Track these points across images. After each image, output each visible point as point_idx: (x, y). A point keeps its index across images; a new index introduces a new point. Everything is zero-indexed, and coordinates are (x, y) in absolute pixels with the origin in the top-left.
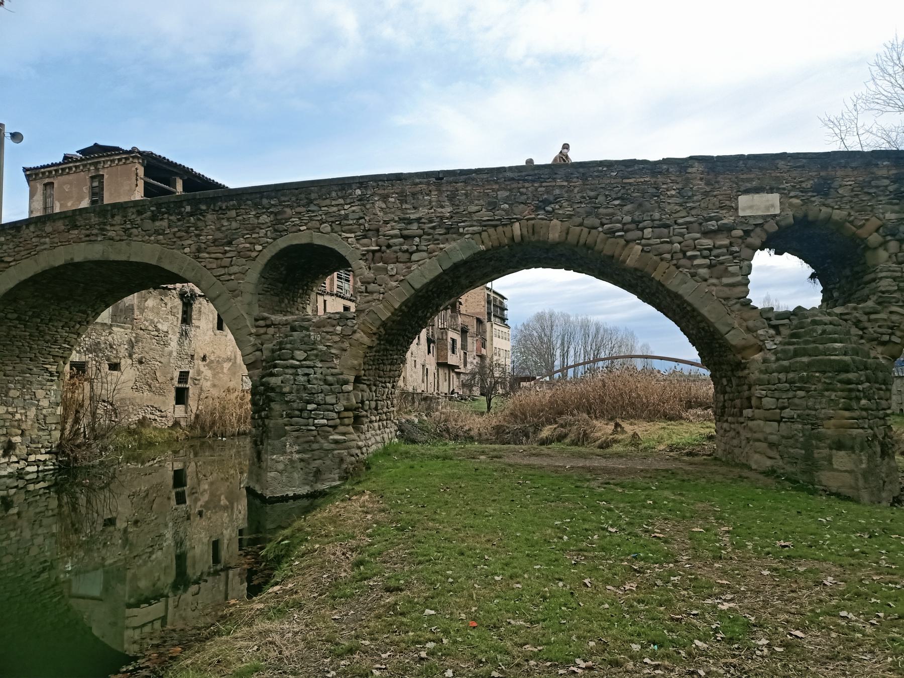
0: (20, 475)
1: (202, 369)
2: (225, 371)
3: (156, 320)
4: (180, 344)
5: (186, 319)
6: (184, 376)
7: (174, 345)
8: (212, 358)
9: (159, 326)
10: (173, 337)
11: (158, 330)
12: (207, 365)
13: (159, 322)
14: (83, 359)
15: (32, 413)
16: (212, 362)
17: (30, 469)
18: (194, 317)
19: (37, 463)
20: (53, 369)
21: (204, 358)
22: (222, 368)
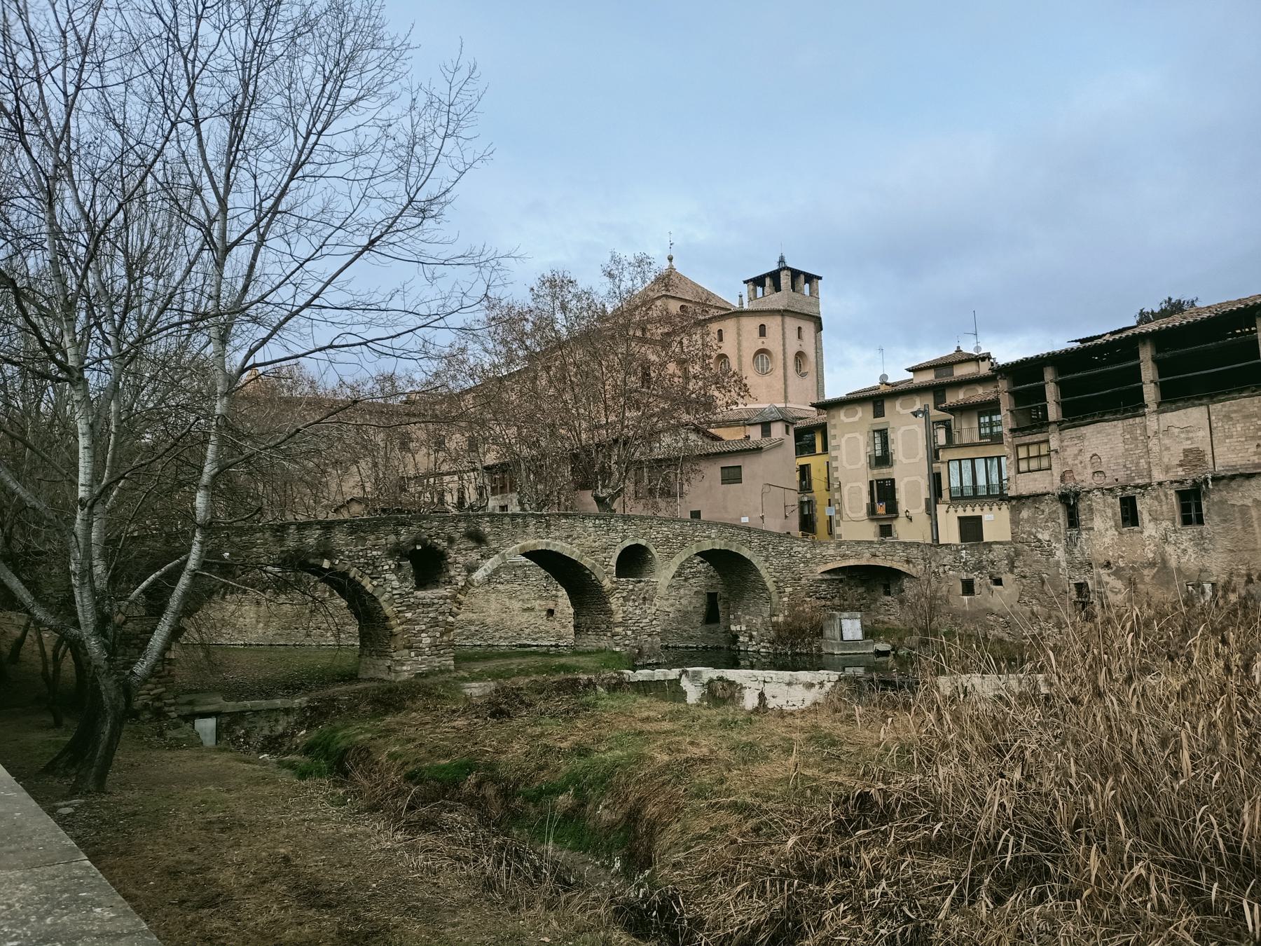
0: (758, 652)
1: (1106, 578)
2: (1147, 579)
3: (1034, 530)
4: (1069, 552)
5: (1073, 521)
6: (1081, 587)
7: (1060, 554)
8: (1121, 564)
9: (1040, 536)
10: (1057, 545)
11: (1039, 540)
12: (1115, 574)
13: (1038, 532)
14: (971, 576)
15: (760, 620)
16: (1123, 569)
17: (762, 650)
18: (1082, 517)
19: (764, 647)
20: (765, 595)
21: (1108, 565)
22: (1142, 576)
